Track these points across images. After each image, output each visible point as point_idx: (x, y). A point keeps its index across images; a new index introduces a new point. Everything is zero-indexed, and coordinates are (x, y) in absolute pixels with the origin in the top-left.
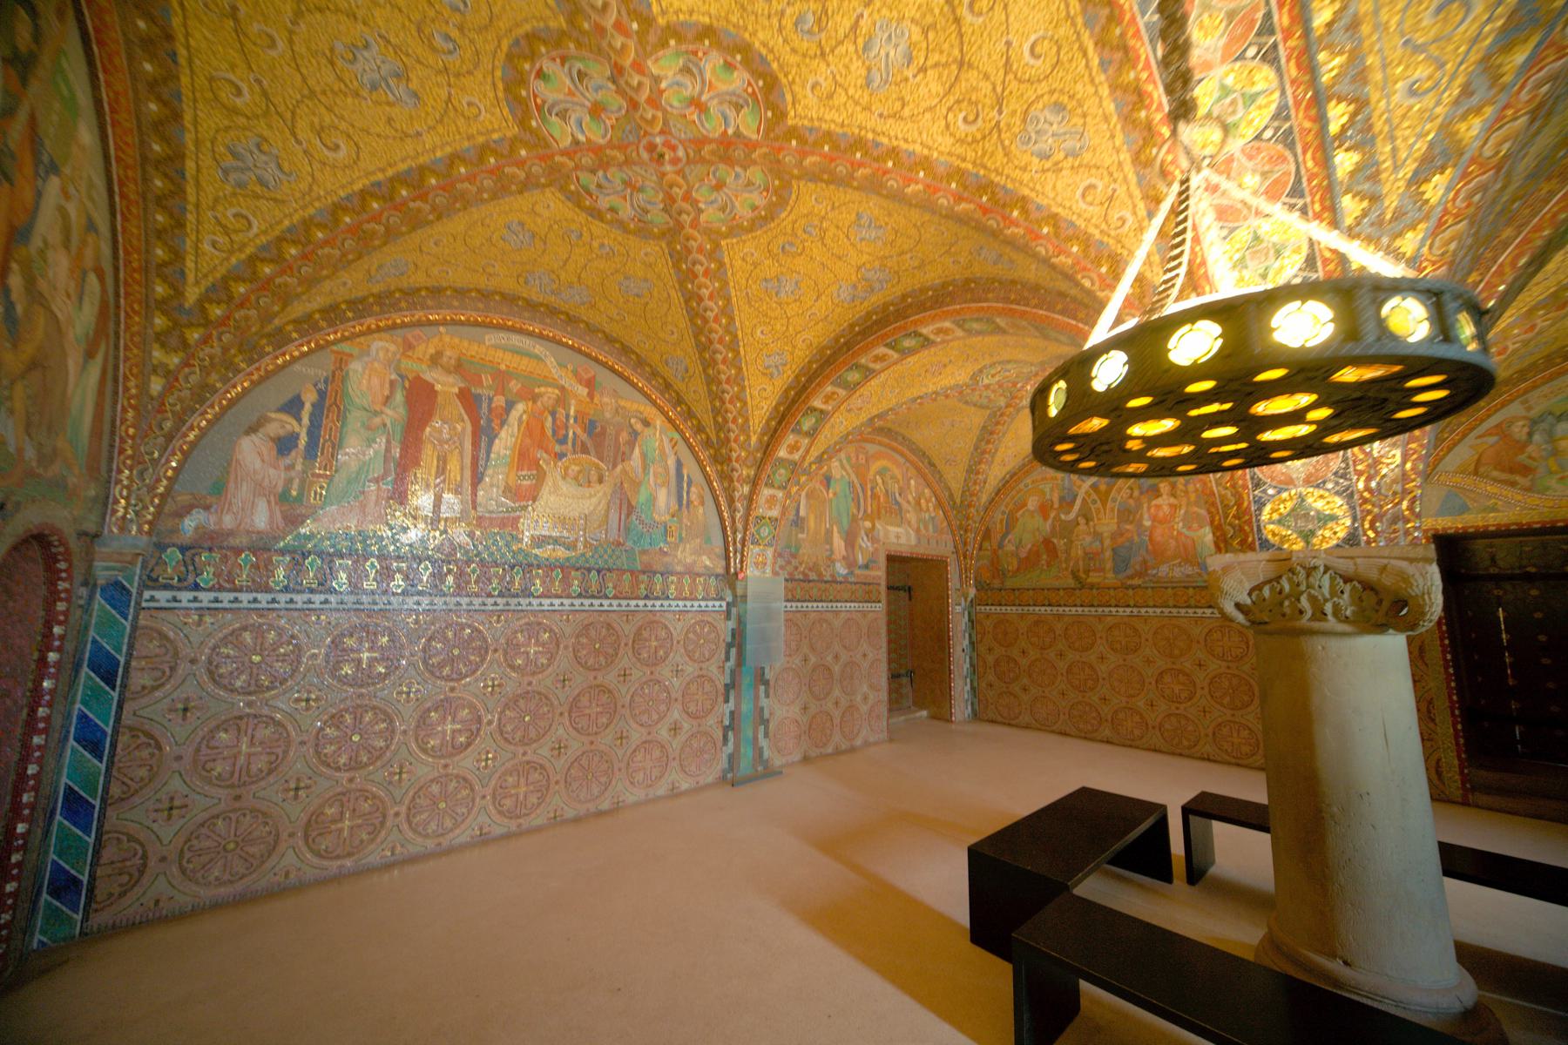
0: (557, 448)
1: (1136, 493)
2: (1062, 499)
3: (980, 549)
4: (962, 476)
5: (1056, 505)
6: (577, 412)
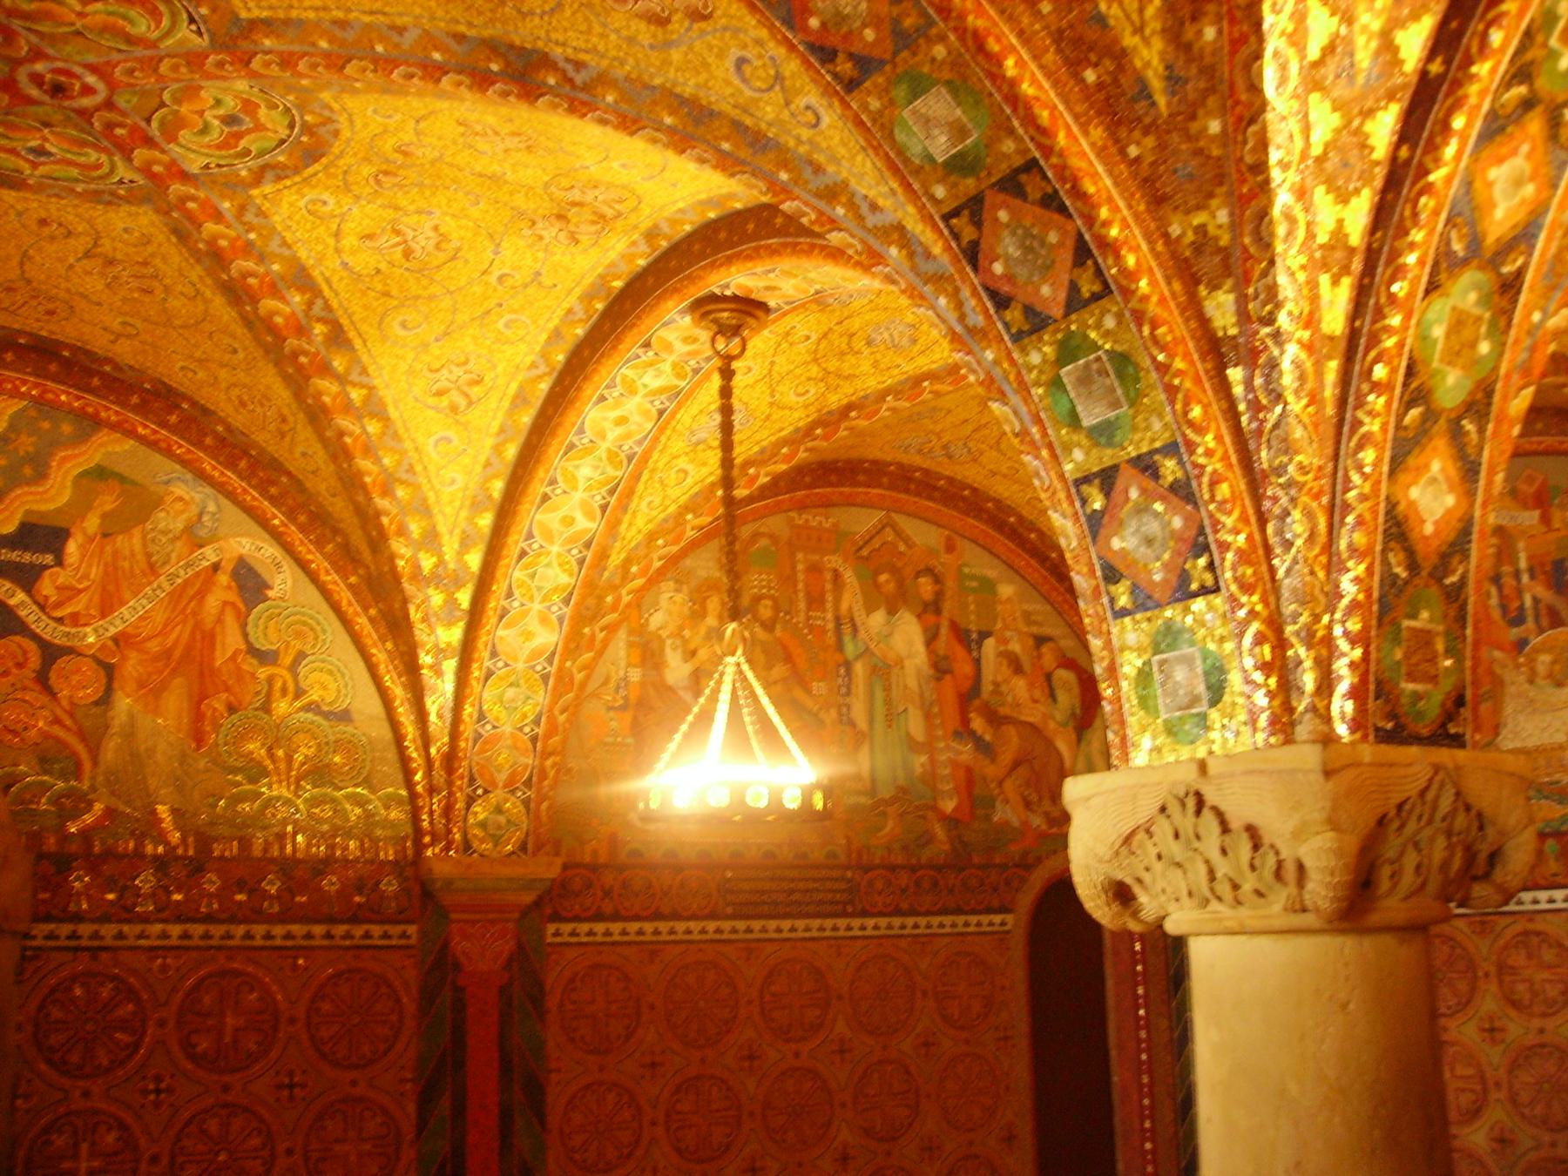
0: (1515, 633)
6: (1530, 558)
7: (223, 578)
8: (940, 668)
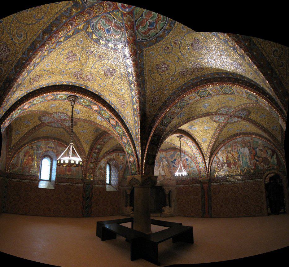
7: (185, 160)
8: (251, 153)
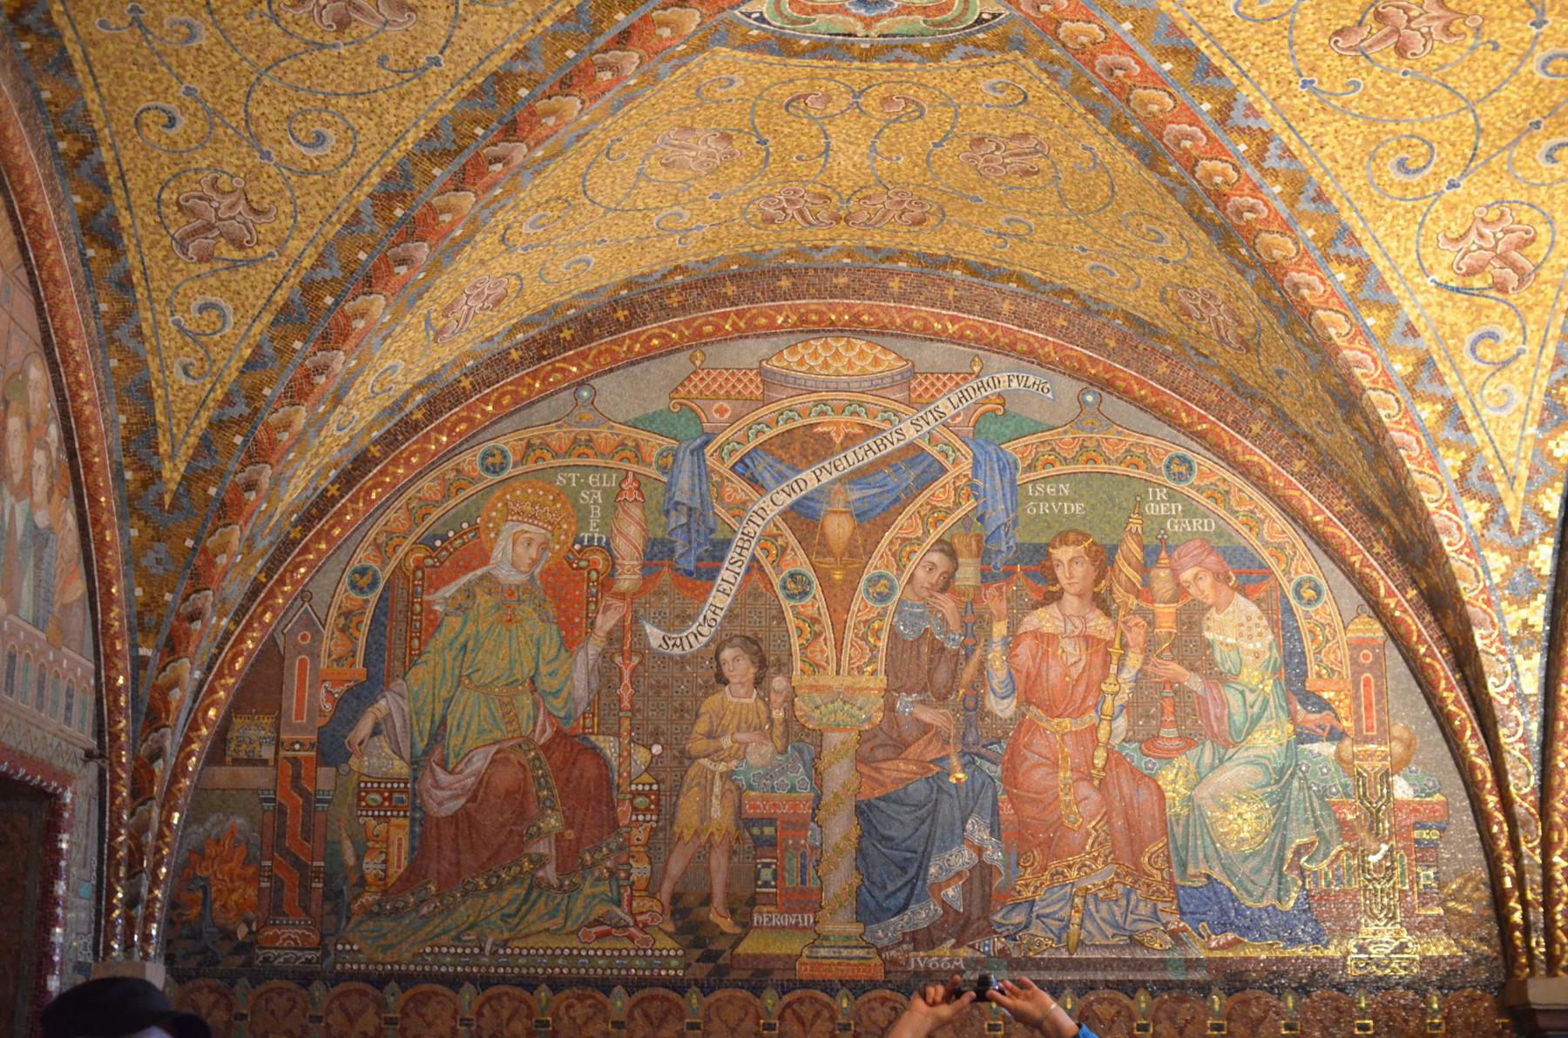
1: (968, 574)
2: (656, 553)
3: (217, 753)
4: (240, 334)
5: (627, 580)
